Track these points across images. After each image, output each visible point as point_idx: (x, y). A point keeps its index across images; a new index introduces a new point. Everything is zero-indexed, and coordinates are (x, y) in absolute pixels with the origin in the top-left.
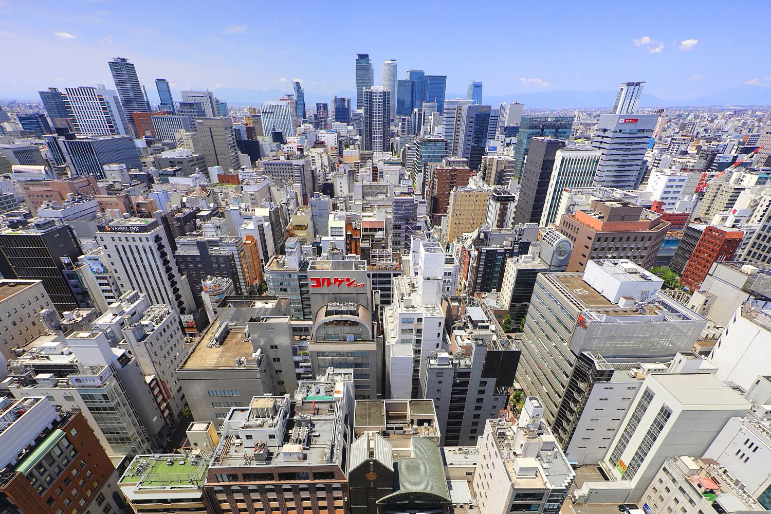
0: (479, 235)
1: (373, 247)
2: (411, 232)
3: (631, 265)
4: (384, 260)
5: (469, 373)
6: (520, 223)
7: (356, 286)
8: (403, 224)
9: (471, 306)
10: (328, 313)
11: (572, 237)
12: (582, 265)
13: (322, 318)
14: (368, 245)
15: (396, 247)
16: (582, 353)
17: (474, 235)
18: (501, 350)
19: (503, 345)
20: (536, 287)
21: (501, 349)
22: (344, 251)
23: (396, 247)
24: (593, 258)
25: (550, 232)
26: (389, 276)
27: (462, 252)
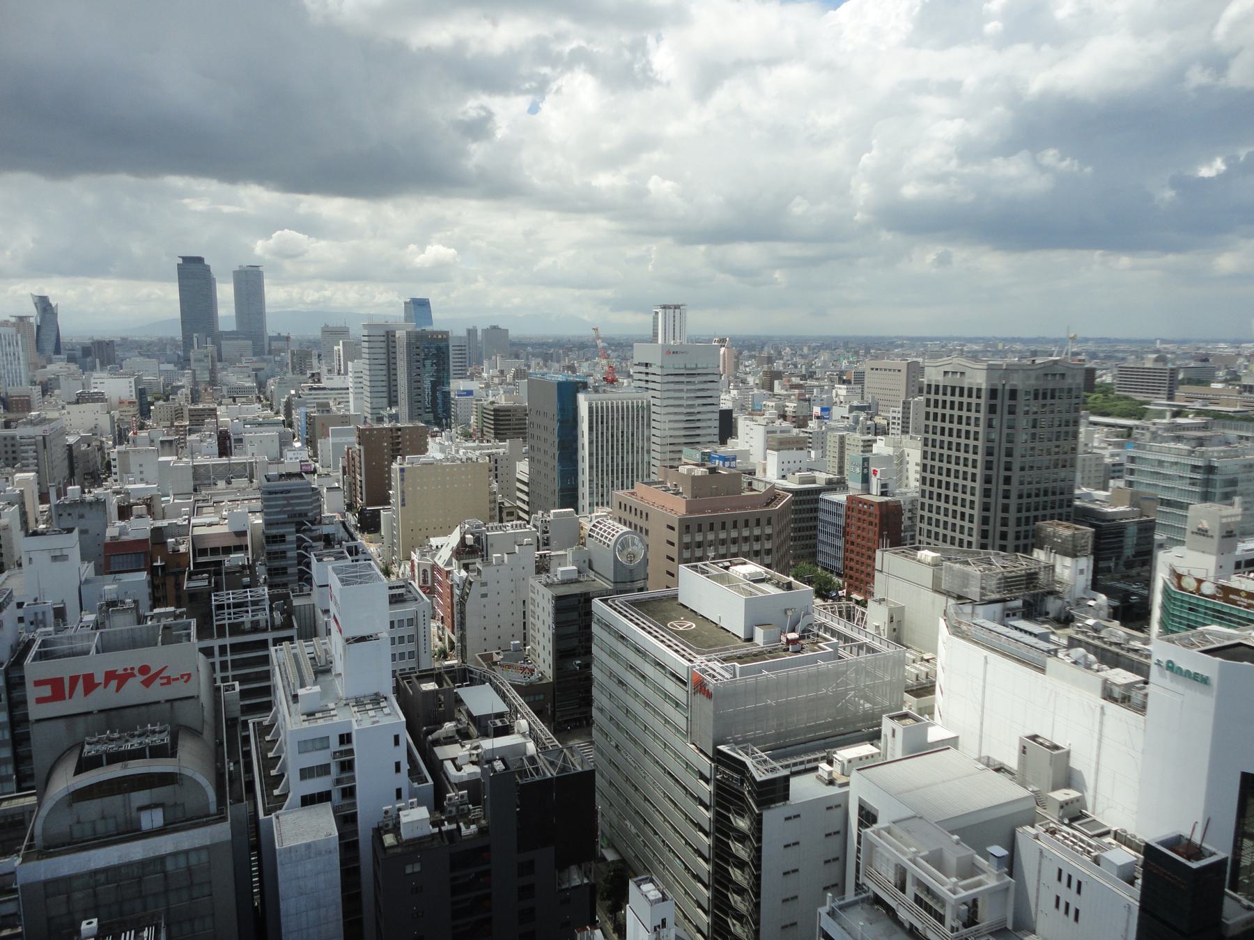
0: (463, 539)
1: (218, 587)
2: (311, 547)
3: (752, 568)
4: (247, 612)
5: (486, 849)
6: (540, 512)
7: (169, 683)
8: (290, 533)
9: (467, 686)
10: (84, 765)
11: (641, 528)
12: (672, 575)
13: (65, 781)
14: (206, 583)
15: (277, 580)
16: (719, 750)
17: (454, 539)
18: (549, 776)
19: (552, 763)
20: (595, 629)
21: (550, 773)
22: (145, 601)
23: (277, 580)
24: (686, 561)
25: (598, 522)
26: (263, 644)
27: (433, 575)
